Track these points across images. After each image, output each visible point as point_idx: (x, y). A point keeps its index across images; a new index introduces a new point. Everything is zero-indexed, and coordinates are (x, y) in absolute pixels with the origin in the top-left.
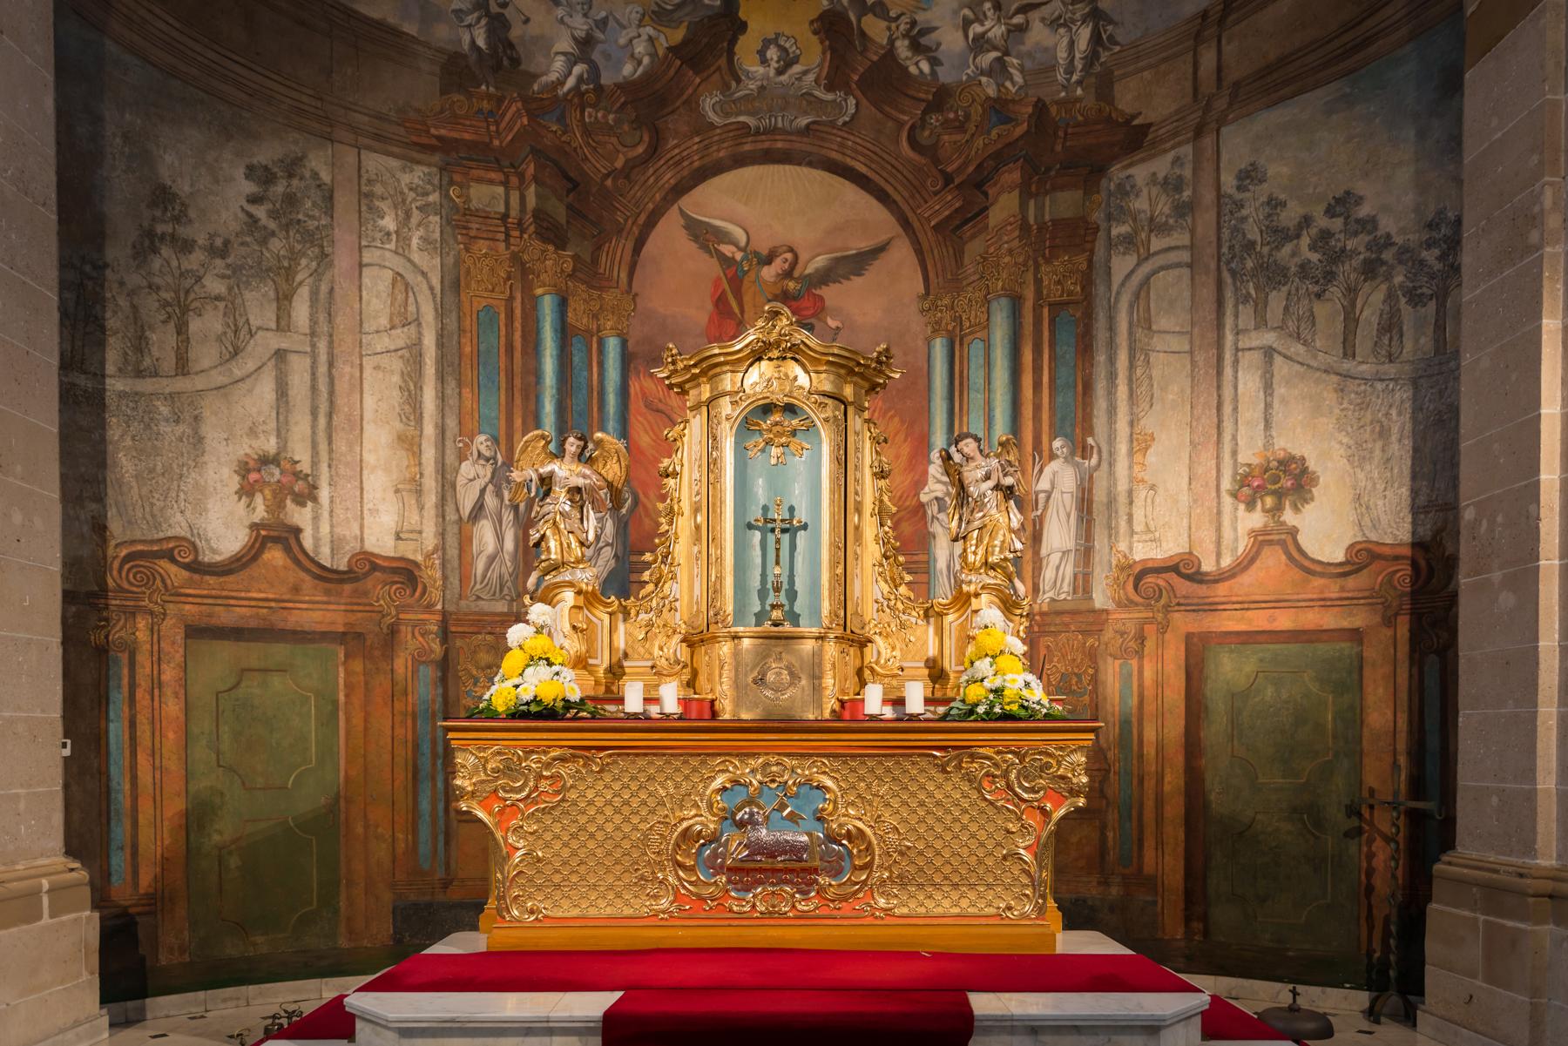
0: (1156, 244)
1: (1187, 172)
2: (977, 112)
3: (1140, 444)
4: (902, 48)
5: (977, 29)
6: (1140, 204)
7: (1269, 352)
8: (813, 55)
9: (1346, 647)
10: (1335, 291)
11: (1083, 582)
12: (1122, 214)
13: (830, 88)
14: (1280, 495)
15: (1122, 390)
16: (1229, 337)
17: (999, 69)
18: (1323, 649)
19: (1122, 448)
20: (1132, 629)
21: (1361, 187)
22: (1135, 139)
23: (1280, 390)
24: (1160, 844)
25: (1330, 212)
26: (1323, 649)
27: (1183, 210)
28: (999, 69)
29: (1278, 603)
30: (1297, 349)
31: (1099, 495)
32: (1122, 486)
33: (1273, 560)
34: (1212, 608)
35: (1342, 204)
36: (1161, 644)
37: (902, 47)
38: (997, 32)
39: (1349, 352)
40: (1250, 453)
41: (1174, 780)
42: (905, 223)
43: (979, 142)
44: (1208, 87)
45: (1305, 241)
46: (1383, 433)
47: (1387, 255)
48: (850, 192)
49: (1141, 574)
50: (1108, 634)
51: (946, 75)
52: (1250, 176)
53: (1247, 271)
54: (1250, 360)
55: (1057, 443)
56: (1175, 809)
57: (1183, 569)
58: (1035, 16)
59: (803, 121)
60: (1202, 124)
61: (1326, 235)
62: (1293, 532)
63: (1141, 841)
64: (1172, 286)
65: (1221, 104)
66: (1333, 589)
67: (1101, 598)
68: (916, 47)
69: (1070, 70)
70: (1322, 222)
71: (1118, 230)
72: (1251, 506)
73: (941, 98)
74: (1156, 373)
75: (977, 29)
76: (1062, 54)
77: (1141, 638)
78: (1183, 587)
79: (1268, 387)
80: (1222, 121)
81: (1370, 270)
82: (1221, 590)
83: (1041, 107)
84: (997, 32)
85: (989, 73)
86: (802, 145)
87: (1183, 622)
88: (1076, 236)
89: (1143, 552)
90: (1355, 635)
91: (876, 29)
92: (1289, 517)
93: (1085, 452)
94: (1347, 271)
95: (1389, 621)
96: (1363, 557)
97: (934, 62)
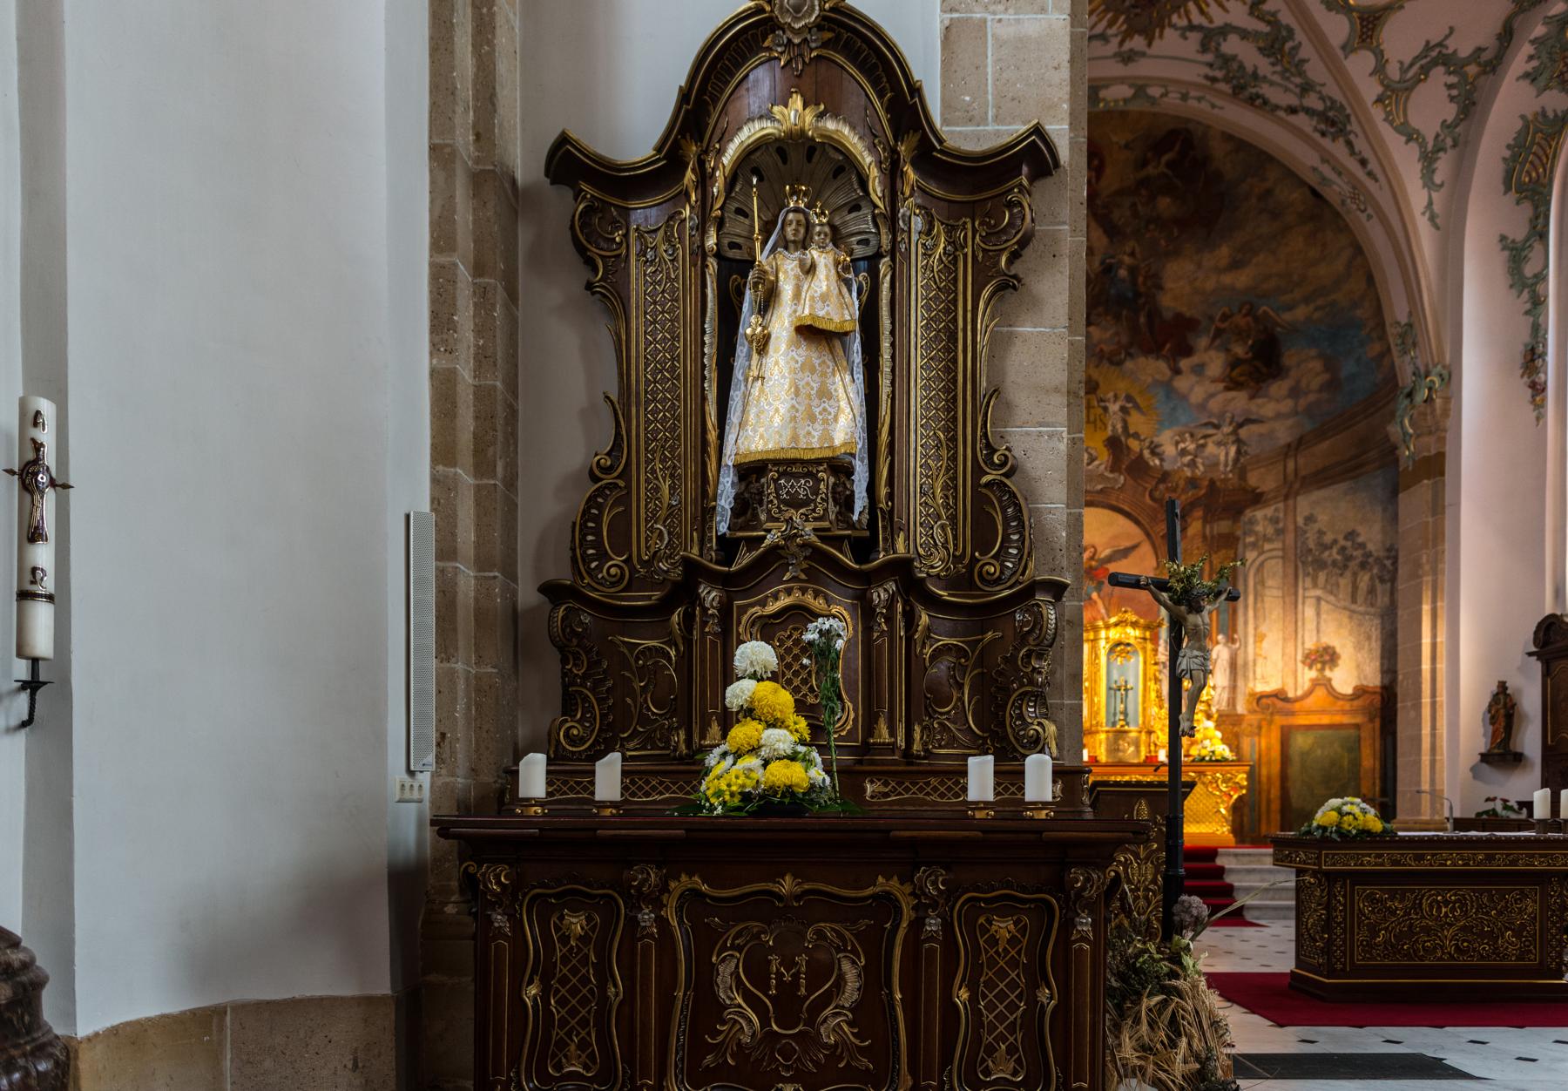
0: (1267, 546)
1: (1281, 515)
2: (1182, 483)
3: (1259, 638)
4: (1146, 453)
5: (1182, 445)
6: (1259, 528)
7: (1319, 599)
8: (1104, 457)
9: (1352, 732)
10: (1348, 574)
11: (1232, 702)
12: (1252, 532)
13: (1112, 471)
14: (1324, 663)
15: (1251, 613)
16: (1300, 591)
17: (1192, 464)
18: (1343, 733)
19: (1251, 640)
20: (1255, 723)
21: (1360, 529)
22: (1257, 499)
23: (1324, 616)
24: (1269, 822)
25: (1346, 538)
26: (1343, 733)
27: (1280, 532)
28: (1192, 464)
29: (1323, 712)
30: (1331, 598)
31: (1240, 662)
32: (1251, 657)
33: (1320, 692)
34: (1292, 713)
35: (1351, 535)
36: (1269, 730)
37: (1146, 453)
38: (1192, 447)
39: (1354, 601)
40: (1310, 644)
41: (1275, 793)
42: (1148, 535)
43: (1183, 497)
44: (1291, 477)
45: (1335, 550)
46: (1369, 638)
47: (1371, 560)
48: (1121, 520)
49: (1260, 698)
50: (1244, 725)
51: (1167, 466)
52: (1310, 519)
53: (1310, 562)
54: (1310, 603)
55: (1220, 637)
56: (1276, 806)
57: (1279, 696)
58: (1210, 440)
59: (1099, 487)
60: (1289, 491)
61: (1343, 549)
62: (1330, 680)
64: (1275, 567)
65: (1297, 486)
66: (1347, 706)
67: (1241, 708)
68: (1153, 453)
69: (1226, 465)
70: (1342, 542)
71: (1250, 539)
72: (1310, 667)
73: (1165, 476)
74: (1267, 606)
75: (1182, 445)
76: (1222, 458)
77: (1260, 728)
78: (1280, 704)
79: (1318, 614)
80: (1297, 494)
81: (1363, 565)
82: (1297, 706)
83: (1212, 482)
84: (1192, 447)
85: (1188, 465)
86: (1099, 498)
87: (1280, 720)
88: (1229, 542)
89: (1260, 688)
90: (1357, 726)
91: (1134, 445)
92: (1328, 673)
93: (1233, 641)
94: (1353, 565)
95: (1371, 720)
96: (1360, 692)
97: (1162, 460)
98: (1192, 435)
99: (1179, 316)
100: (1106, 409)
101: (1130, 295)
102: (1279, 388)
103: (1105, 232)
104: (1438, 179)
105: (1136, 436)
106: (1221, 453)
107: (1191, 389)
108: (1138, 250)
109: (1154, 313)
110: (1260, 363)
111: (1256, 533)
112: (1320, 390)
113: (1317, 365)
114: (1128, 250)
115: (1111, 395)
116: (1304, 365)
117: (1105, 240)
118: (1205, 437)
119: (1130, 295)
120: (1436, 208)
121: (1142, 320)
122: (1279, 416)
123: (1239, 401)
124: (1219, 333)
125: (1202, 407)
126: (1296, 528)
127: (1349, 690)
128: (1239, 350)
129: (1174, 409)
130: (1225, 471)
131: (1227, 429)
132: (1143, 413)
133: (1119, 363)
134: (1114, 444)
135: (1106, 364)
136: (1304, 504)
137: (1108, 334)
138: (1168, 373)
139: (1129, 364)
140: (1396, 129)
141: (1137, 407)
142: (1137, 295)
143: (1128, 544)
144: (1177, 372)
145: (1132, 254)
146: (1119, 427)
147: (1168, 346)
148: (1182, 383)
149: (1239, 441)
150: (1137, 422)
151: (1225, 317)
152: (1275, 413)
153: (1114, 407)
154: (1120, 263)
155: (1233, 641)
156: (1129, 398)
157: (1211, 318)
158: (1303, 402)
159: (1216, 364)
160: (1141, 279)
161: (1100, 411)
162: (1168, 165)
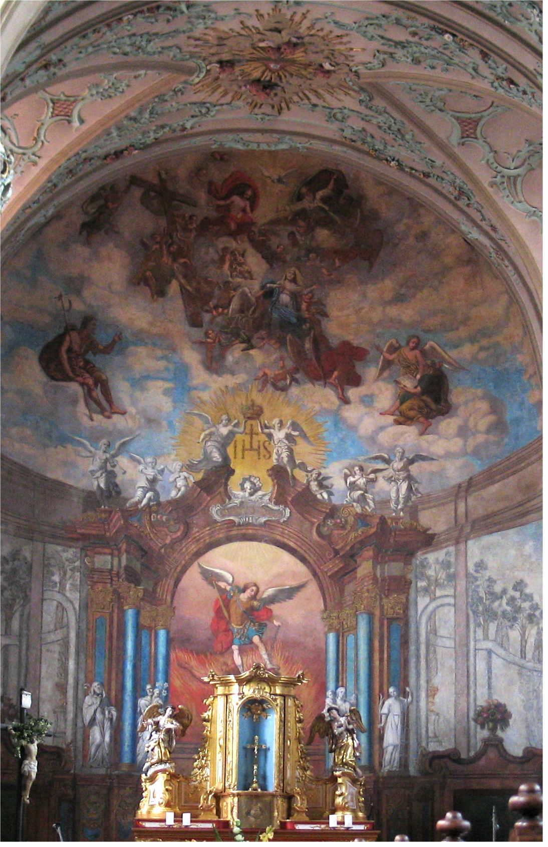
1: (452, 560)
4: (314, 486)
8: (268, 488)
10: (517, 626)
13: (276, 504)
17: (362, 499)
22: (428, 541)
28: (362, 499)
37: (314, 486)
38: (361, 481)
43: (352, 535)
48: (286, 557)
51: (336, 500)
52: (480, 566)
58: (380, 475)
61: (513, 599)
62: (501, 741)
65: (468, 529)
68: (321, 486)
69: (397, 503)
70: (511, 592)
71: (422, 584)
72: (483, 727)
73: (333, 512)
76: (393, 495)
83: (383, 520)
84: (361, 481)
91: (300, 475)
97: (330, 494)
98: (361, 469)
102: (448, 425)
105: (303, 466)
107: (360, 420)
109: (320, 340)
111: (428, 578)
114: (290, 276)
115: (276, 421)
117: (265, 266)
118: (375, 471)
119: (294, 320)
121: (308, 345)
122: (448, 455)
124: (388, 364)
126: (467, 575)
128: (409, 384)
131: (397, 465)
139: (294, 391)
141: (304, 436)
142: (301, 320)
144: (346, 401)
145: (294, 281)
146: (285, 455)
147: (336, 373)
148: (351, 413)
149: (409, 478)
150: (303, 450)
151: (393, 349)
154: (282, 289)
157: (378, 348)
158: (471, 443)
160: (304, 306)
161: (263, 438)
162: (324, 200)
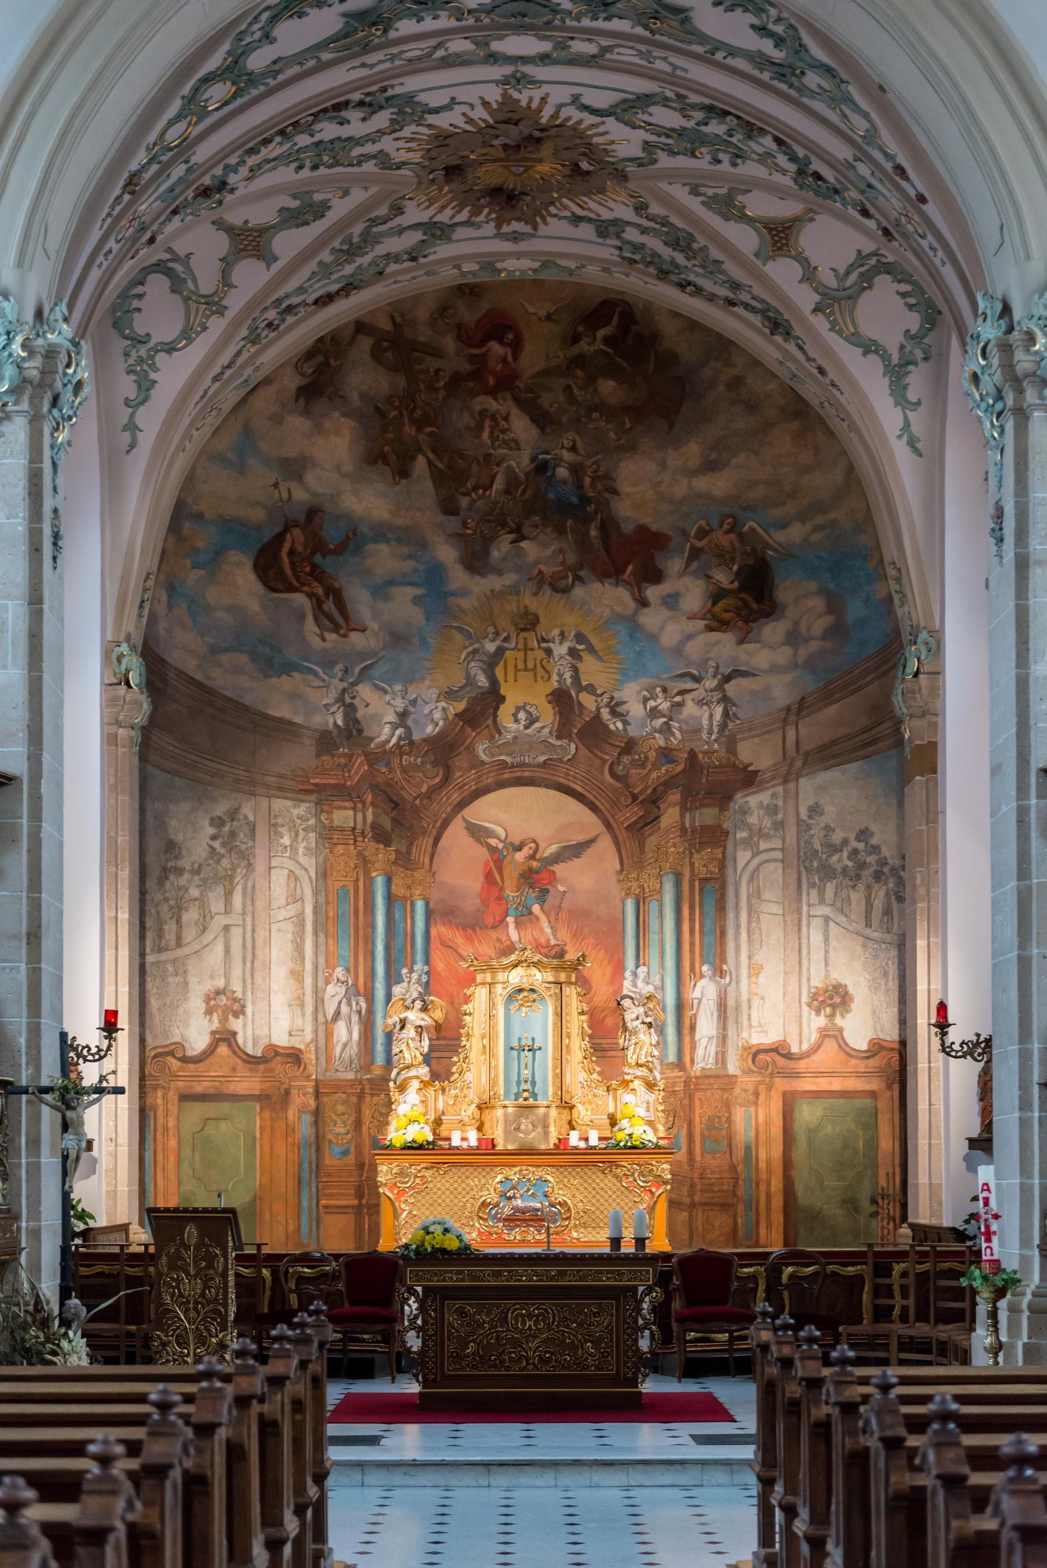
0: (763, 846)
2: (652, 754)
3: (755, 970)
4: (605, 714)
5: (651, 704)
6: (753, 820)
7: (827, 919)
9: (868, 1102)
10: (861, 886)
13: (559, 737)
14: (834, 1007)
15: (744, 936)
16: (805, 909)
18: (858, 1103)
19: (744, 973)
20: (751, 1088)
21: (873, 828)
22: (750, 779)
23: (833, 943)
25: (858, 839)
26: (858, 1103)
29: (832, 1074)
30: (841, 919)
31: (731, 1002)
32: (744, 997)
33: (830, 1047)
34: (796, 1075)
36: (769, 1097)
37: (605, 714)
38: (665, 706)
39: (868, 924)
40: (817, 982)
41: (777, 1184)
42: (608, 825)
43: (654, 775)
44: (791, 752)
46: (885, 975)
47: (886, 870)
48: (572, 805)
49: (756, 1052)
50: (737, 1091)
51: (633, 732)
52: (815, 810)
53: (815, 867)
54: (817, 922)
55: (705, 968)
56: (778, 1202)
57: (780, 1050)
58: (688, 697)
61: (855, 852)
62: (841, 1030)
63: (758, 1223)
64: (773, 873)
65: (799, 764)
66: (862, 1066)
67: (733, 1067)
68: (614, 713)
69: (710, 733)
72: (818, 1012)
73: (629, 746)
74: (764, 926)
75: (651, 704)
76: (705, 722)
77: (757, 1094)
78: (781, 1062)
79: (826, 940)
80: (799, 776)
81: (878, 876)
82: (802, 1065)
83: (692, 755)
84: (665, 706)
86: (541, 774)
87: (781, 1084)
88: (715, 837)
89: (757, 1039)
90: (873, 1094)
91: (588, 701)
92: (839, 1021)
93: (722, 974)
94: (867, 874)
95: (889, 1087)
96: (877, 1047)
97: (626, 723)
98: (665, 690)
99: (642, 529)
100: (549, 652)
101: (575, 500)
102: (773, 631)
103: (534, 420)
104: (912, 396)
105: (591, 689)
106: (702, 715)
107: (662, 627)
108: (579, 444)
109: (609, 525)
110: (750, 596)
111: (749, 827)
112: (824, 637)
113: (818, 603)
115: (556, 632)
116: (801, 600)
118: (682, 693)
119: (575, 500)
120: (915, 429)
121: (594, 533)
122: (774, 669)
123: (724, 646)
124: (695, 554)
125: (678, 651)
126: (799, 822)
127: (864, 1047)
129: (640, 653)
130: (709, 743)
131: (710, 683)
132: (601, 660)
133: (565, 590)
134: (561, 699)
135: (547, 591)
136: (807, 786)
137: (549, 552)
138: (632, 604)
139: (579, 592)
140: (846, 339)
141: (591, 650)
142: (585, 500)
143: (582, 838)
144: (643, 603)
146: (568, 675)
147: (630, 568)
148: (650, 619)
149: (725, 700)
150: (591, 669)
151: (702, 534)
152: (770, 662)
153: (560, 650)
155: (722, 974)
156: (580, 638)
157: (684, 533)
158: (803, 652)
159: (693, 594)
160: (587, 481)
161: (541, 654)
